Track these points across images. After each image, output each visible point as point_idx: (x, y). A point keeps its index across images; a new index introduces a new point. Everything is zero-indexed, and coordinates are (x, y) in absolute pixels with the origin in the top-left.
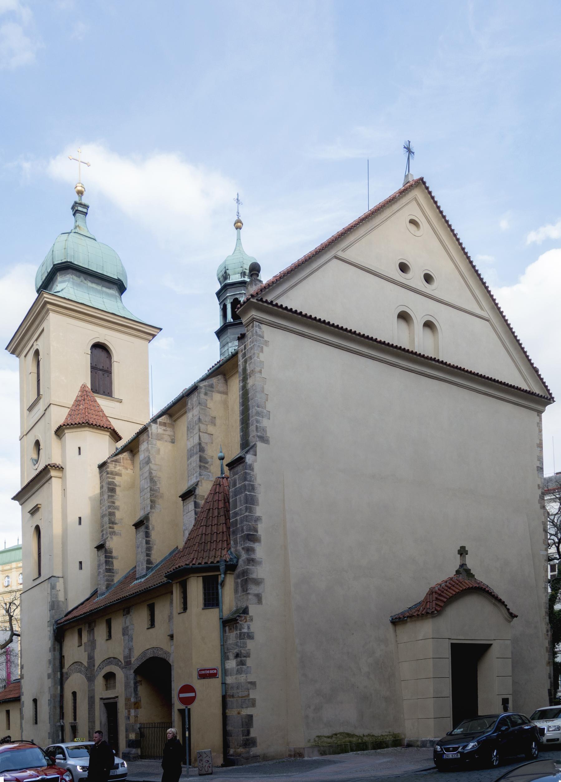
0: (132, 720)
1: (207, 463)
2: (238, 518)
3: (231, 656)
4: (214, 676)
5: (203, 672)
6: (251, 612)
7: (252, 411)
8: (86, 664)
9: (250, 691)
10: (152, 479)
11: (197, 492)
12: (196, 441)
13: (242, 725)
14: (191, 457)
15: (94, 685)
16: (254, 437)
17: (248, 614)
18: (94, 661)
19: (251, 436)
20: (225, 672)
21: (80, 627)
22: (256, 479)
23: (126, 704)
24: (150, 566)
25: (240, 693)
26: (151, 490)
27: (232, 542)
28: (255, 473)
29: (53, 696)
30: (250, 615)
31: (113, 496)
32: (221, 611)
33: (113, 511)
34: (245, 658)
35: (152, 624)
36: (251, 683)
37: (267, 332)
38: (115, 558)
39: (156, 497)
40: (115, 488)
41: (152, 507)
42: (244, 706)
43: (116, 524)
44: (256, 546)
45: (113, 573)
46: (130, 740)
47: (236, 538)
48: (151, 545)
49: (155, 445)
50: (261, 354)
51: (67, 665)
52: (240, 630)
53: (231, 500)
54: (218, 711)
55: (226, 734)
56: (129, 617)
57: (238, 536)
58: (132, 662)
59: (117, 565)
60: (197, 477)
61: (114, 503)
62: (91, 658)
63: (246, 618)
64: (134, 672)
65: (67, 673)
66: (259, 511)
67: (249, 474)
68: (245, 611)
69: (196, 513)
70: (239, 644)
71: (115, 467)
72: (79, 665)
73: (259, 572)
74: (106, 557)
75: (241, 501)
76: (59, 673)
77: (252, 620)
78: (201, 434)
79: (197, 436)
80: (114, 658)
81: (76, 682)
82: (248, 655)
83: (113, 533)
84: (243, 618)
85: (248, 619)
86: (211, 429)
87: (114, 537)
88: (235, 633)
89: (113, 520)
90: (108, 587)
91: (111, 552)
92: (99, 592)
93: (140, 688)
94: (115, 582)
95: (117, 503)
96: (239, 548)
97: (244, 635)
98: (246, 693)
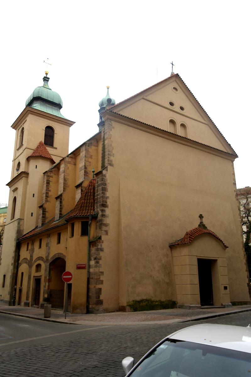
0: (47, 287)
1: (88, 173)
2: (99, 197)
3: (92, 258)
4: (84, 268)
5: (79, 266)
6: (103, 239)
7: (107, 153)
8: (29, 259)
9: (101, 276)
12: (83, 164)
13: (96, 293)
15: (32, 270)
17: (101, 239)
18: (33, 258)
19: (106, 163)
20: (89, 266)
21: (28, 242)
22: (107, 181)
23: (45, 280)
24: (61, 216)
25: (96, 277)
26: (64, 184)
27: (96, 207)
28: (106, 178)
29: (13, 274)
30: (102, 240)
32: (89, 237)
34: (99, 260)
35: (59, 242)
36: (101, 272)
37: (114, 124)
38: (47, 212)
39: (66, 187)
41: (64, 191)
43: (48, 197)
44: (106, 209)
46: (45, 298)
48: (62, 207)
49: (67, 165)
50: (111, 132)
52: (97, 247)
54: (85, 285)
55: (88, 297)
57: (98, 204)
59: (47, 215)
60: (83, 179)
61: (48, 188)
62: (31, 256)
63: (100, 241)
64: (50, 264)
65: (20, 263)
66: (108, 194)
67: (104, 178)
68: (100, 238)
69: (81, 194)
70: (96, 253)
71: (50, 174)
72: (26, 260)
73: (107, 221)
74: (43, 211)
75: (100, 189)
76: (17, 263)
80: (41, 257)
81: (24, 268)
82: (100, 259)
84: (99, 241)
85: (101, 241)
86: (90, 160)
88: (95, 248)
89: (47, 195)
90: (43, 224)
91: (45, 209)
92: (38, 226)
94: (46, 222)
96: (99, 210)
97: (99, 249)
98: (99, 277)
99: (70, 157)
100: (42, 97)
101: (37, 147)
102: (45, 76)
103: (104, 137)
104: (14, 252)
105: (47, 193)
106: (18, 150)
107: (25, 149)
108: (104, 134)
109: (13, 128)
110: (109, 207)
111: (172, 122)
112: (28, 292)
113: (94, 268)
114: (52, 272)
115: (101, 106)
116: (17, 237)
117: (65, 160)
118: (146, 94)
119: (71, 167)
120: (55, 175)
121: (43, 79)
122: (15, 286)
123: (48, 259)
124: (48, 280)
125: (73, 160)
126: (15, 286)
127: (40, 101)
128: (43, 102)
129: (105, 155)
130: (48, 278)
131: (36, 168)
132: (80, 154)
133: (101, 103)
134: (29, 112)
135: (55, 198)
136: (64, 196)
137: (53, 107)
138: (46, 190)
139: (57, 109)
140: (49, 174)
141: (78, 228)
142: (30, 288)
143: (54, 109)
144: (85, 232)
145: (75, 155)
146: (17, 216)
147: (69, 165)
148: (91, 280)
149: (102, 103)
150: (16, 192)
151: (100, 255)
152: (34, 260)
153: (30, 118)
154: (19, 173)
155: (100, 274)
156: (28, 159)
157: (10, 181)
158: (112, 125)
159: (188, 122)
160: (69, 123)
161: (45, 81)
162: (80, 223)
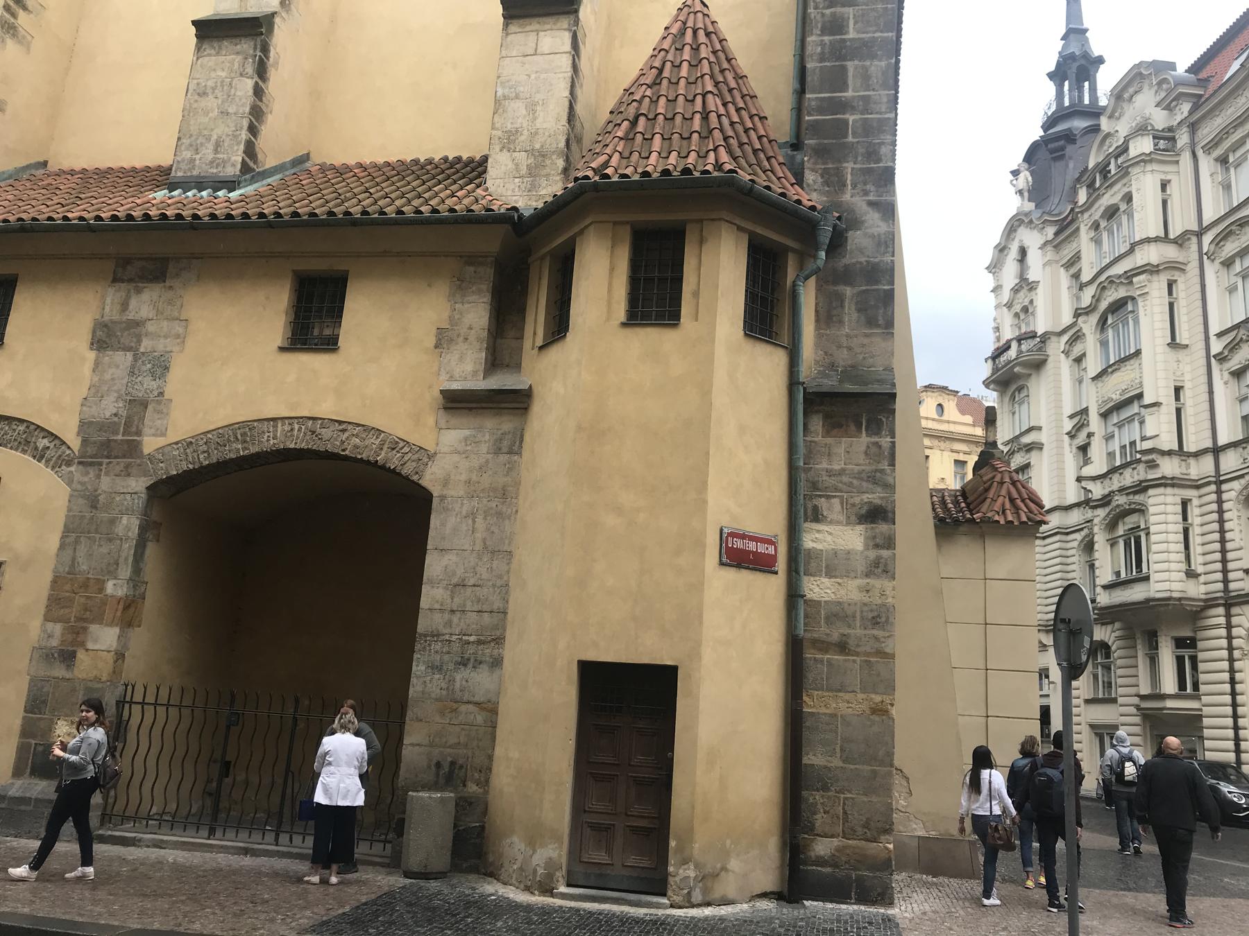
2: (851, 118)
4: (762, 564)
5: (739, 544)
47: (839, 173)
93: (151, 550)
113: (867, 576)
144: (765, 316)
148: (809, 654)
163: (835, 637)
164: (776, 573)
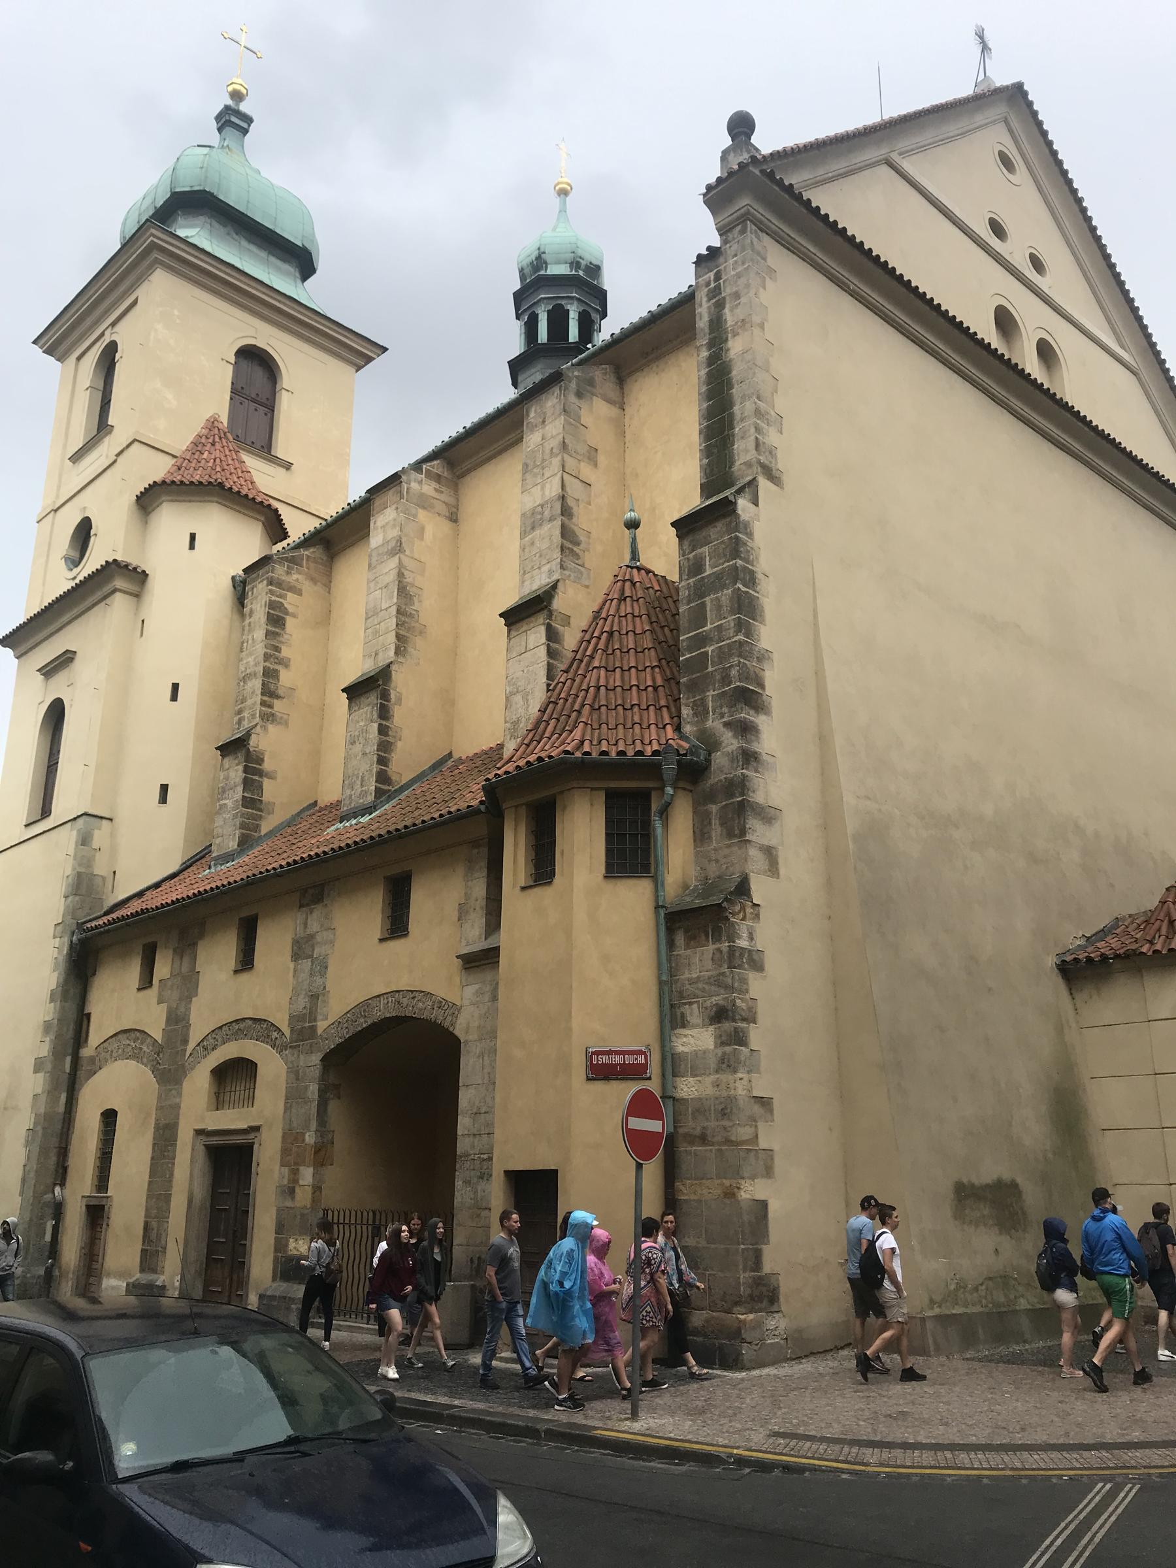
0: (303, 1197)
1: (578, 544)
2: (710, 649)
3: (693, 1014)
5: (605, 1059)
8: (158, 1036)
9: (761, 1124)
10: (405, 588)
11: (557, 604)
12: (552, 489)
14: (533, 528)
15: (180, 1094)
16: (748, 464)
18: (187, 1026)
19: (738, 463)
23: (285, 1151)
24: (386, 787)
26: (398, 612)
31: (278, 634)
33: (276, 667)
34: (744, 1025)
38: (271, 776)
40: (284, 619)
41: (398, 652)
42: (746, 1175)
43: (278, 697)
44: (761, 720)
45: (261, 810)
47: (703, 701)
48: (391, 739)
49: (415, 516)
51: (95, 1037)
53: (682, 609)
56: (318, 912)
58: (319, 1032)
59: (270, 792)
60: (551, 572)
62: (178, 1021)
63: (743, 909)
65: (92, 1060)
66: (767, 636)
68: (743, 889)
74: (246, 770)
75: (719, 607)
76: (68, 1059)
77: (757, 916)
78: (566, 476)
79: (556, 481)
81: (118, 1084)
83: (269, 717)
84: (738, 908)
85: (749, 910)
86: (586, 471)
87: (271, 727)
88: (711, 947)
90: (245, 843)
91: (260, 761)
94: (264, 830)
95: (285, 652)
96: (714, 724)
99: (429, 475)
100: (221, 197)
101: (195, 444)
102: (230, 102)
103: (717, 323)
104: (52, 999)
105: (270, 675)
106: (76, 457)
107: (128, 446)
108: (720, 305)
109: (49, 352)
110: (774, 714)
111: (1004, 320)
112: (154, 1224)
113: (717, 1072)
114: (333, 1106)
115: (527, 271)
116: (71, 912)
117: (405, 486)
118: (904, 144)
119: (433, 526)
120: (314, 581)
121: (218, 118)
122: (57, 1190)
123: (313, 1029)
124: (309, 1156)
125: (444, 489)
126: (57, 1190)
127: (211, 217)
128: (225, 226)
129: (731, 416)
130: (310, 1138)
131: (192, 546)
132: (520, 440)
133: (536, 253)
134: (155, 255)
135: (501, 615)
136: (401, 681)
137: (272, 259)
138: (267, 657)
139: (288, 274)
140: (279, 571)
141: (583, 831)
142: (168, 1198)
143: (279, 269)
144: (630, 854)
145: (451, 464)
146: (65, 804)
147: (422, 515)
148: (683, 1147)
149: (539, 258)
150: (61, 677)
151: (747, 991)
152: (196, 1034)
153: (160, 290)
154: (81, 578)
155: (757, 1109)
156: (148, 500)
157: (22, 620)
158: (765, 259)
159: (1066, 341)
160: (357, 350)
161: (228, 130)
162: (601, 797)
163: (698, 1132)
164: (650, 1078)
